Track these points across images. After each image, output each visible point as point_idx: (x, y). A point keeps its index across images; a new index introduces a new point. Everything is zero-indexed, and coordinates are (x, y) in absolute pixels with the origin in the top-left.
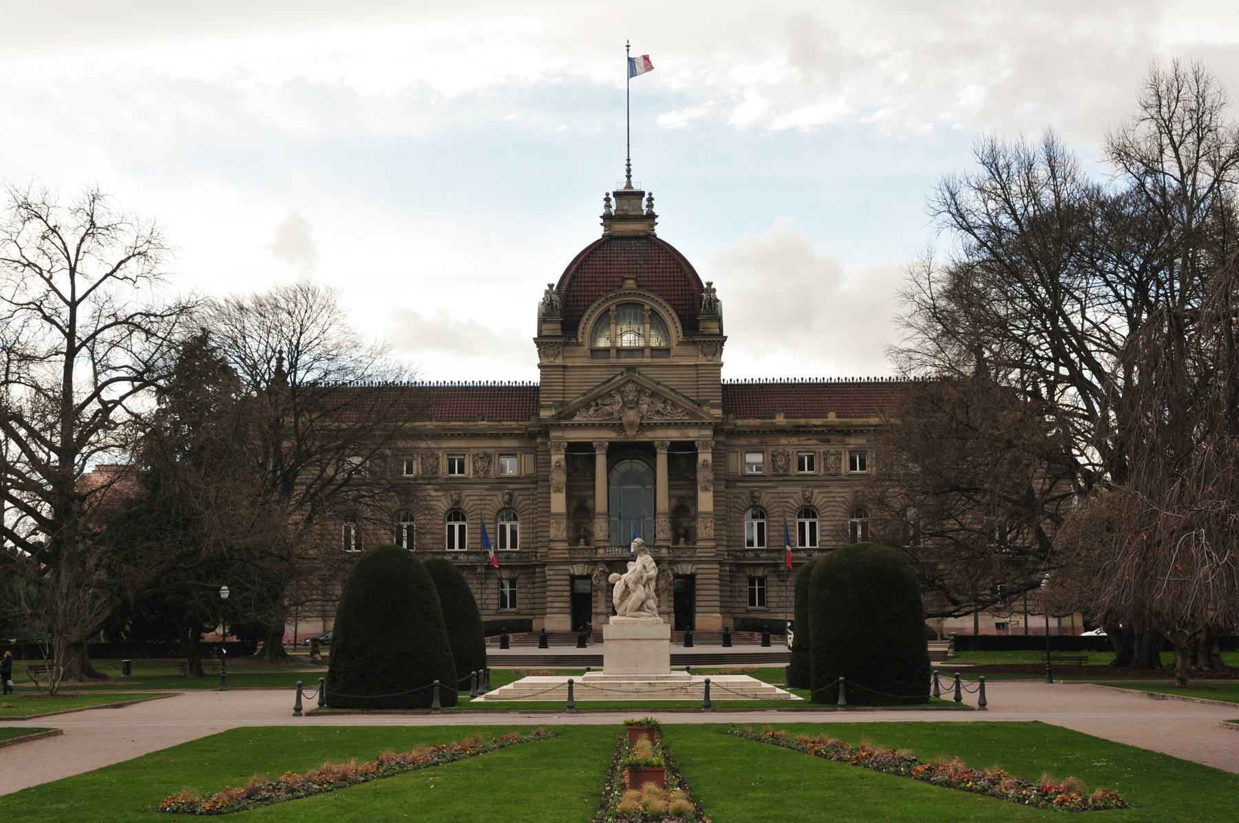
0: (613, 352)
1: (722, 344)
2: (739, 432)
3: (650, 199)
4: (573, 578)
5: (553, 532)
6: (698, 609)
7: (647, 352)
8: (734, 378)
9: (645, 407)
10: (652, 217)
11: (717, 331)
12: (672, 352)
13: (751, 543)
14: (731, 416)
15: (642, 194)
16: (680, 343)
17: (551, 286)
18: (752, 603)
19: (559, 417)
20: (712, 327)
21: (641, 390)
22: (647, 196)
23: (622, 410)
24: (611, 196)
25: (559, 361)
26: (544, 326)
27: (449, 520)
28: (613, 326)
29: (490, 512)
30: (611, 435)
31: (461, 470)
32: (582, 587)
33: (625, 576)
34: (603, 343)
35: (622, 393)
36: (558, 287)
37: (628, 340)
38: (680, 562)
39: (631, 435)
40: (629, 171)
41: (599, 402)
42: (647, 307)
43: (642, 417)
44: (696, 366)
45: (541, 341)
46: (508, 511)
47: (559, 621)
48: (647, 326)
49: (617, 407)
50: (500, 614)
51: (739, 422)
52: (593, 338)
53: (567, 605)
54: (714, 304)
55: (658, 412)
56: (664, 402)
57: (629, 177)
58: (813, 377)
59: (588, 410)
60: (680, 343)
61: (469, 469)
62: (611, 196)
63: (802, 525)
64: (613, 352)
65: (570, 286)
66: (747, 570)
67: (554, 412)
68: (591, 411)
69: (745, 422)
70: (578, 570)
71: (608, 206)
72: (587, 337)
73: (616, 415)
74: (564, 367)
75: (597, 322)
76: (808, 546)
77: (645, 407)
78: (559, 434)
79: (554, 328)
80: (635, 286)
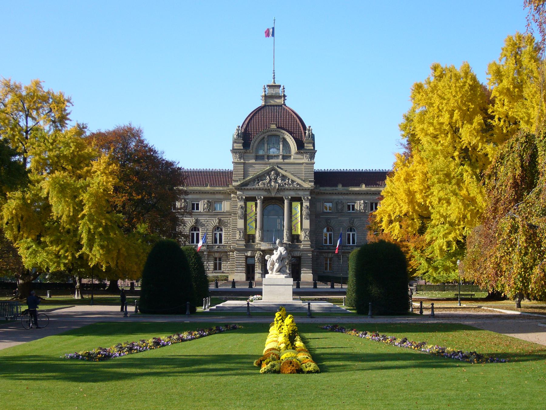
0: (266, 157)
1: (315, 154)
2: (321, 193)
3: (284, 88)
4: (247, 257)
5: (238, 237)
6: (302, 272)
7: (281, 157)
8: (320, 169)
10: (285, 96)
11: (312, 148)
12: (292, 157)
13: (326, 242)
14: (318, 186)
15: (280, 86)
16: (297, 153)
17: (239, 127)
18: (326, 269)
19: (242, 185)
20: (309, 146)
21: (277, 174)
22: (282, 88)
24: (266, 87)
25: (242, 161)
26: (235, 145)
27: (192, 230)
28: (266, 145)
29: (211, 227)
30: (265, 194)
31: (198, 209)
32: (250, 261)
33: (272, 256)
34: (261, 153)
36: (242, 127)
37: (273, 151)
38: (294, 251)
39: (273, 195)
40: (274, 76)
41: (259, 179)
45: (234, 151)
46: (218, 228)
47: (240, 276)
48: (281, 146)
49: (268, 181)
50: (215, 273)
51: (321, 188)
52: (257, 151)
53: (244, 269)
54: (312, 137)
55: (285, 184)
56: (289, 179)
57: (274, 78)
58: (355, 169)
59: (254, 183)
60: (297, 153)
61: (201, 209)
62: (266, 87)
63: (349, 235)
64: (266, 157)
65: (247, 127)
66: (324, 254)
67: (239, 183)
69: (324, 188)
70: (249, 254)
71: (265, 91)
72: (254, 150)
74: (244, 163)
75: (259, 143)
76: (351, 244)
77: (280, 181)
79: (239, 146)
80: (276, 127)
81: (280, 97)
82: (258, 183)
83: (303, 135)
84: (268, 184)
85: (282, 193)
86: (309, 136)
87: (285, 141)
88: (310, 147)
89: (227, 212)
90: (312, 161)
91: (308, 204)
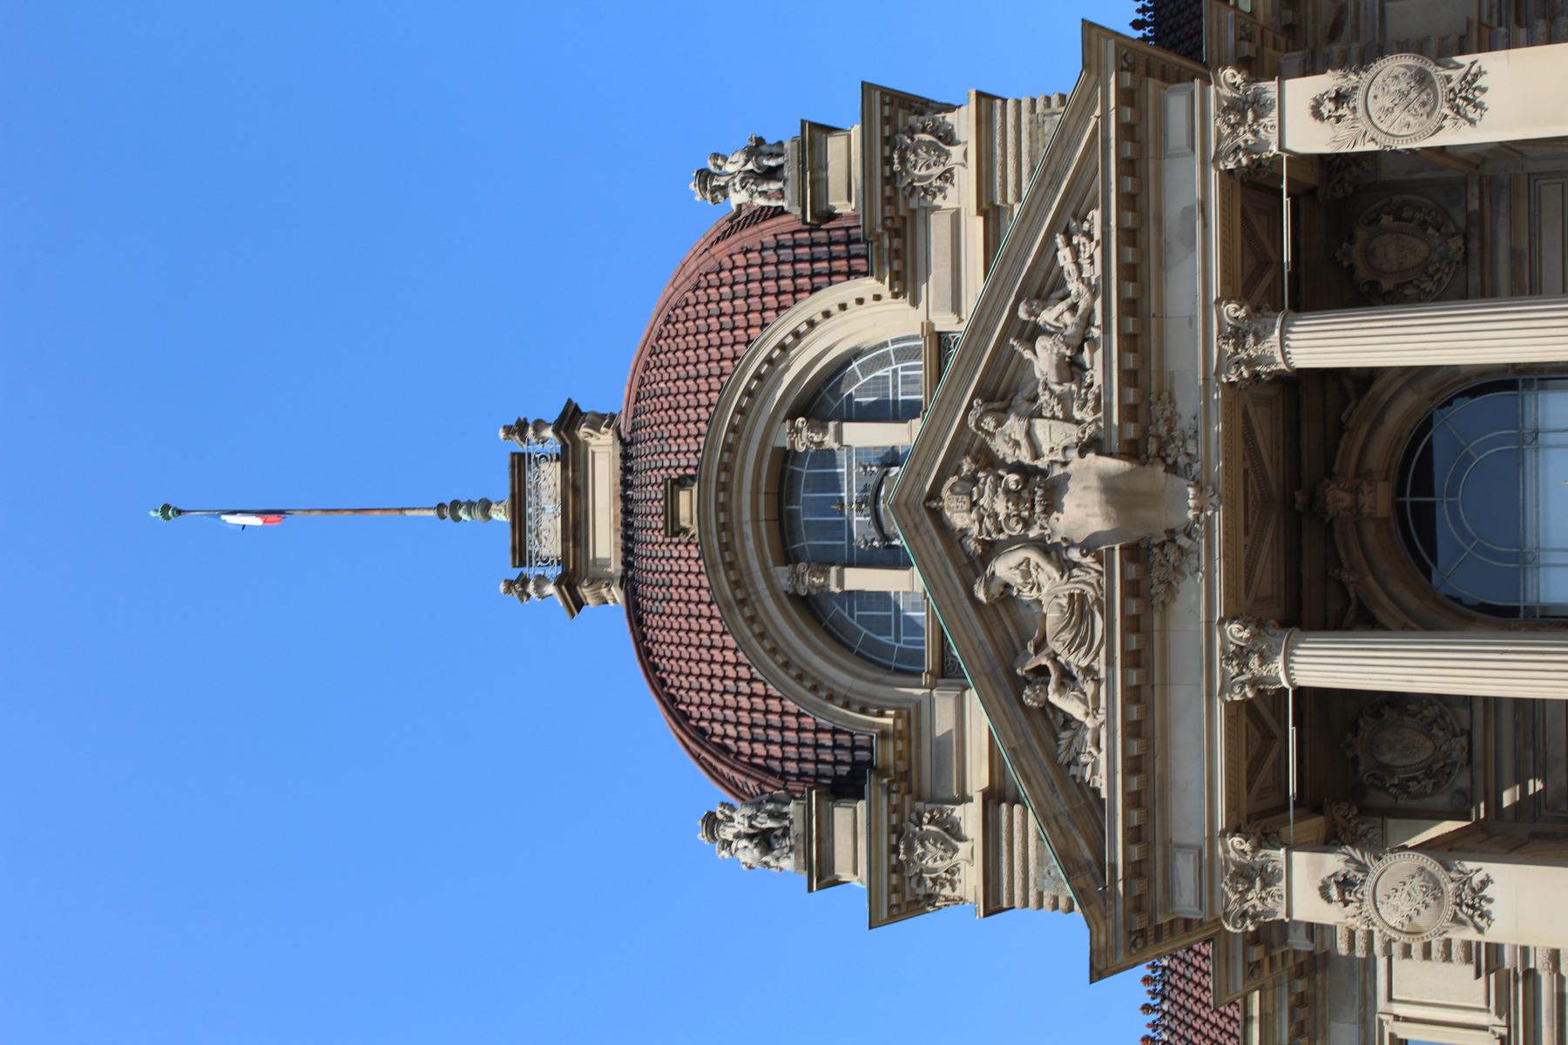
3: (520, 428)
9: (1052, 436)
10: (570, 419)
15: (519, 463)
16: (906, 282)
23: (1051, 551)
25: (969, 817)
26: (842, 869)
28: (859, 579)
35: (991, 549)
40: (470, 506)
42: (783, 439)
43: (1084, 448)
44: (990, 212)
55: (1072, 368)
56: (1032, 333)
59: (1068, 720)
62: (514, 574)
68: (1070, 705)
73: (1088, 578)
74: (995, 797)
77: (1052, 436)
78: (1185, 868)
79: (849, 825)
81: (573, 460)
82: (1067, 679)
83: (767, 231)
84: (1065, 567)
85: (1188, 404)
86: (771, 174)
87: (822, 400)
88: (843, 157)
89: (1503, 1008)
90: (963, 122)
91: (1301, 91)
